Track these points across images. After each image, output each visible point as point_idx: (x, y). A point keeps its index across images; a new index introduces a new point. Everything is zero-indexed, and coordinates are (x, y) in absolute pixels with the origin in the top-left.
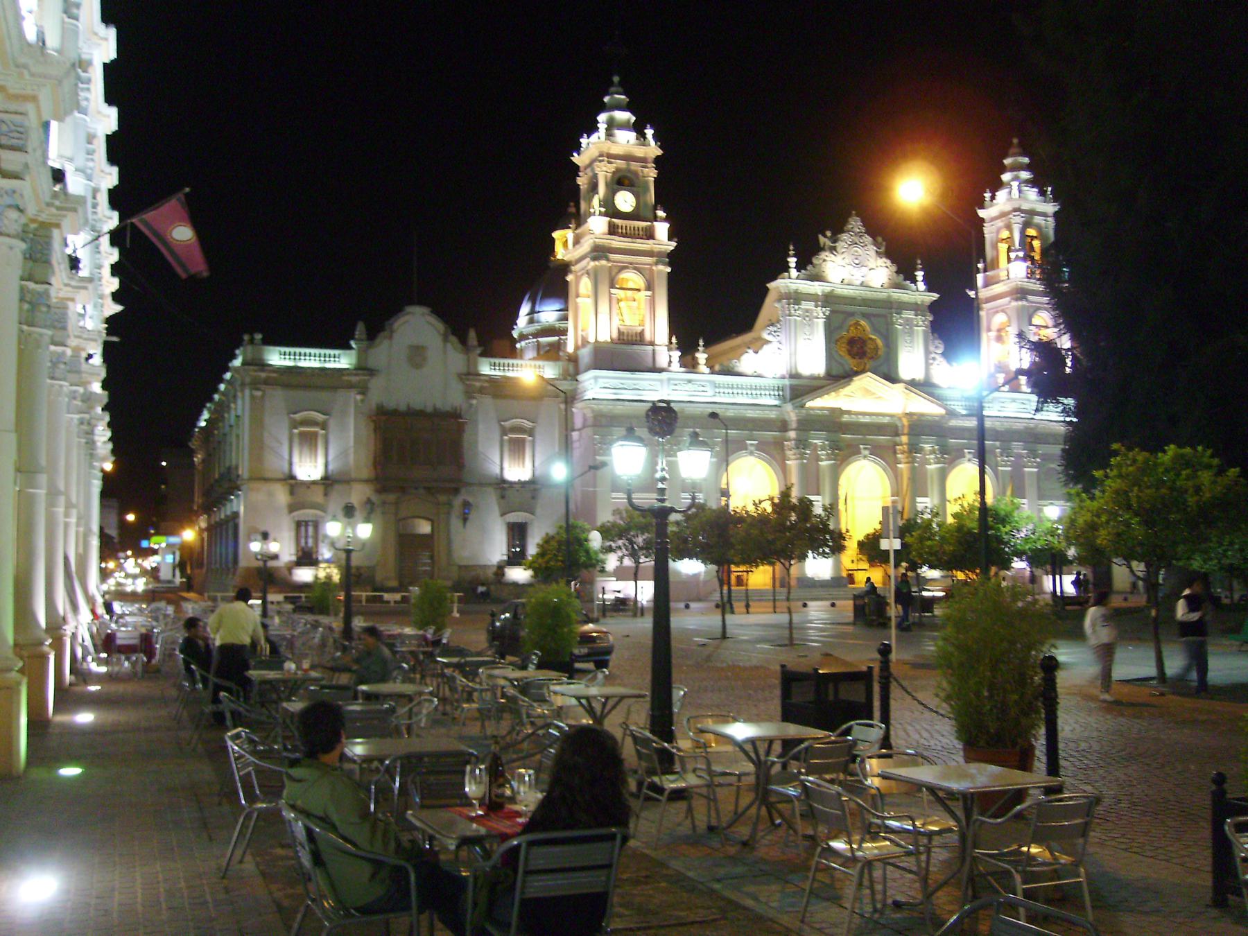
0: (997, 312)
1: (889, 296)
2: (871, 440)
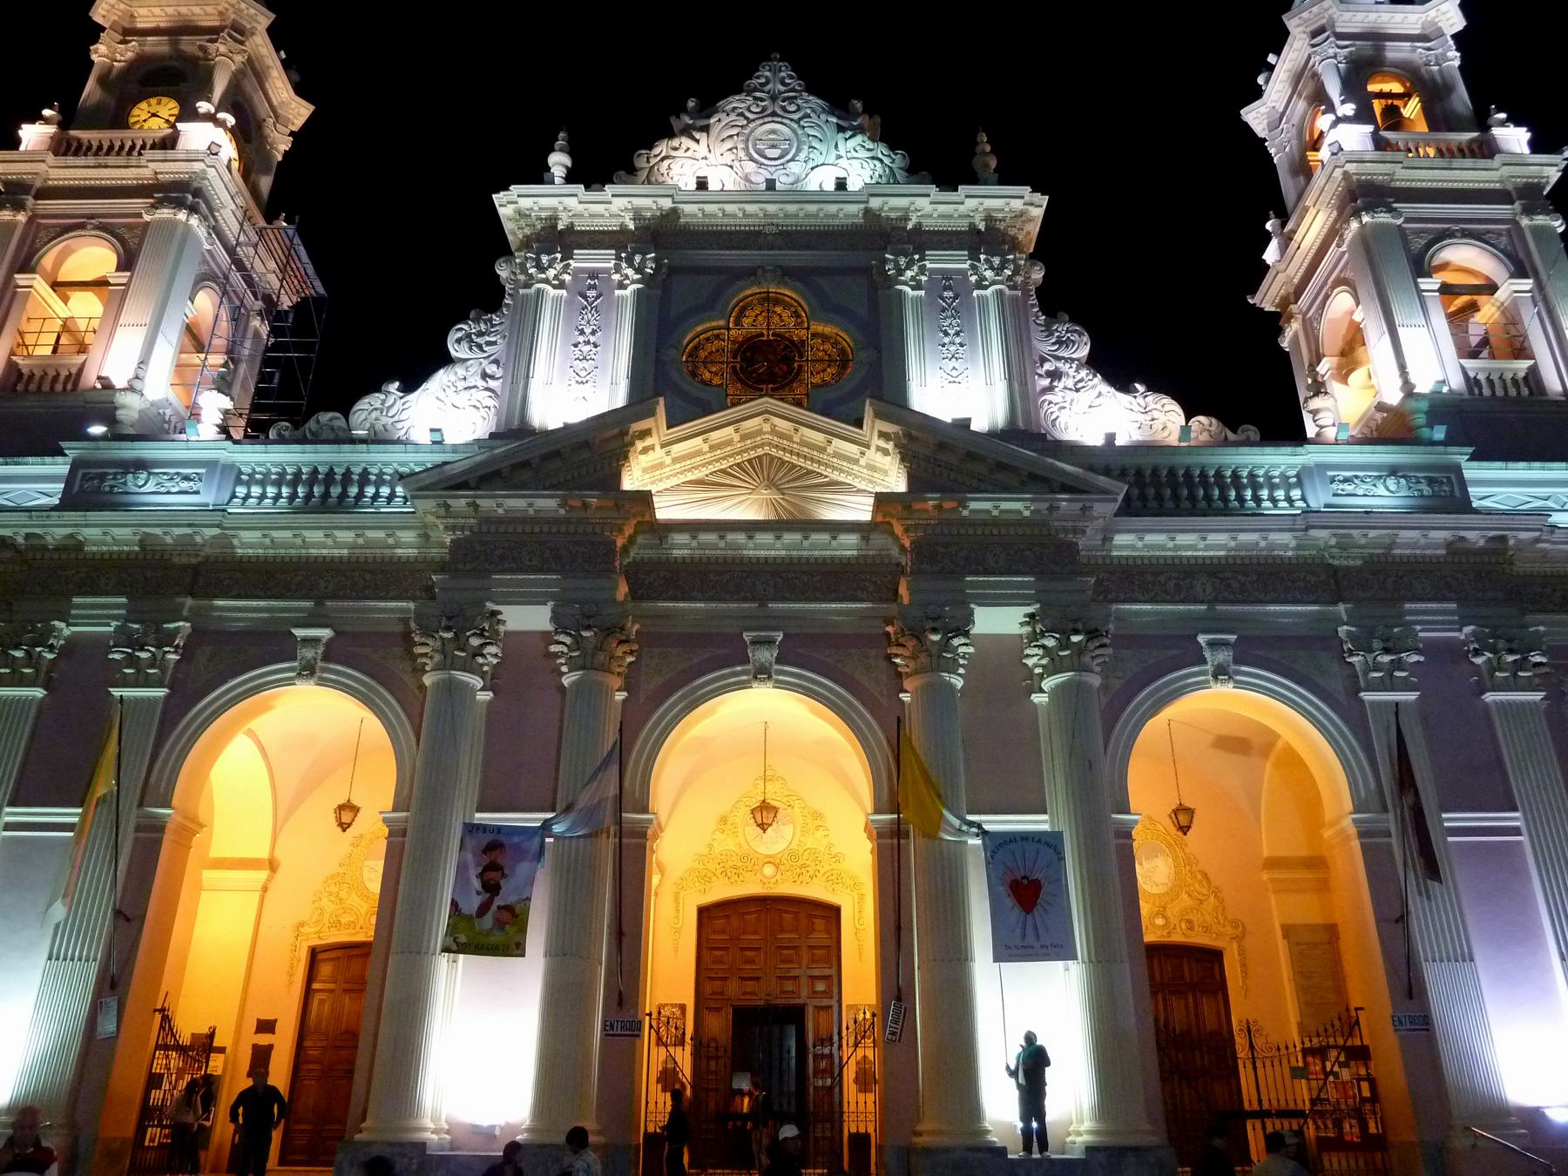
0: (1327, 297)
1: (867, 211)
2: (794, 616)
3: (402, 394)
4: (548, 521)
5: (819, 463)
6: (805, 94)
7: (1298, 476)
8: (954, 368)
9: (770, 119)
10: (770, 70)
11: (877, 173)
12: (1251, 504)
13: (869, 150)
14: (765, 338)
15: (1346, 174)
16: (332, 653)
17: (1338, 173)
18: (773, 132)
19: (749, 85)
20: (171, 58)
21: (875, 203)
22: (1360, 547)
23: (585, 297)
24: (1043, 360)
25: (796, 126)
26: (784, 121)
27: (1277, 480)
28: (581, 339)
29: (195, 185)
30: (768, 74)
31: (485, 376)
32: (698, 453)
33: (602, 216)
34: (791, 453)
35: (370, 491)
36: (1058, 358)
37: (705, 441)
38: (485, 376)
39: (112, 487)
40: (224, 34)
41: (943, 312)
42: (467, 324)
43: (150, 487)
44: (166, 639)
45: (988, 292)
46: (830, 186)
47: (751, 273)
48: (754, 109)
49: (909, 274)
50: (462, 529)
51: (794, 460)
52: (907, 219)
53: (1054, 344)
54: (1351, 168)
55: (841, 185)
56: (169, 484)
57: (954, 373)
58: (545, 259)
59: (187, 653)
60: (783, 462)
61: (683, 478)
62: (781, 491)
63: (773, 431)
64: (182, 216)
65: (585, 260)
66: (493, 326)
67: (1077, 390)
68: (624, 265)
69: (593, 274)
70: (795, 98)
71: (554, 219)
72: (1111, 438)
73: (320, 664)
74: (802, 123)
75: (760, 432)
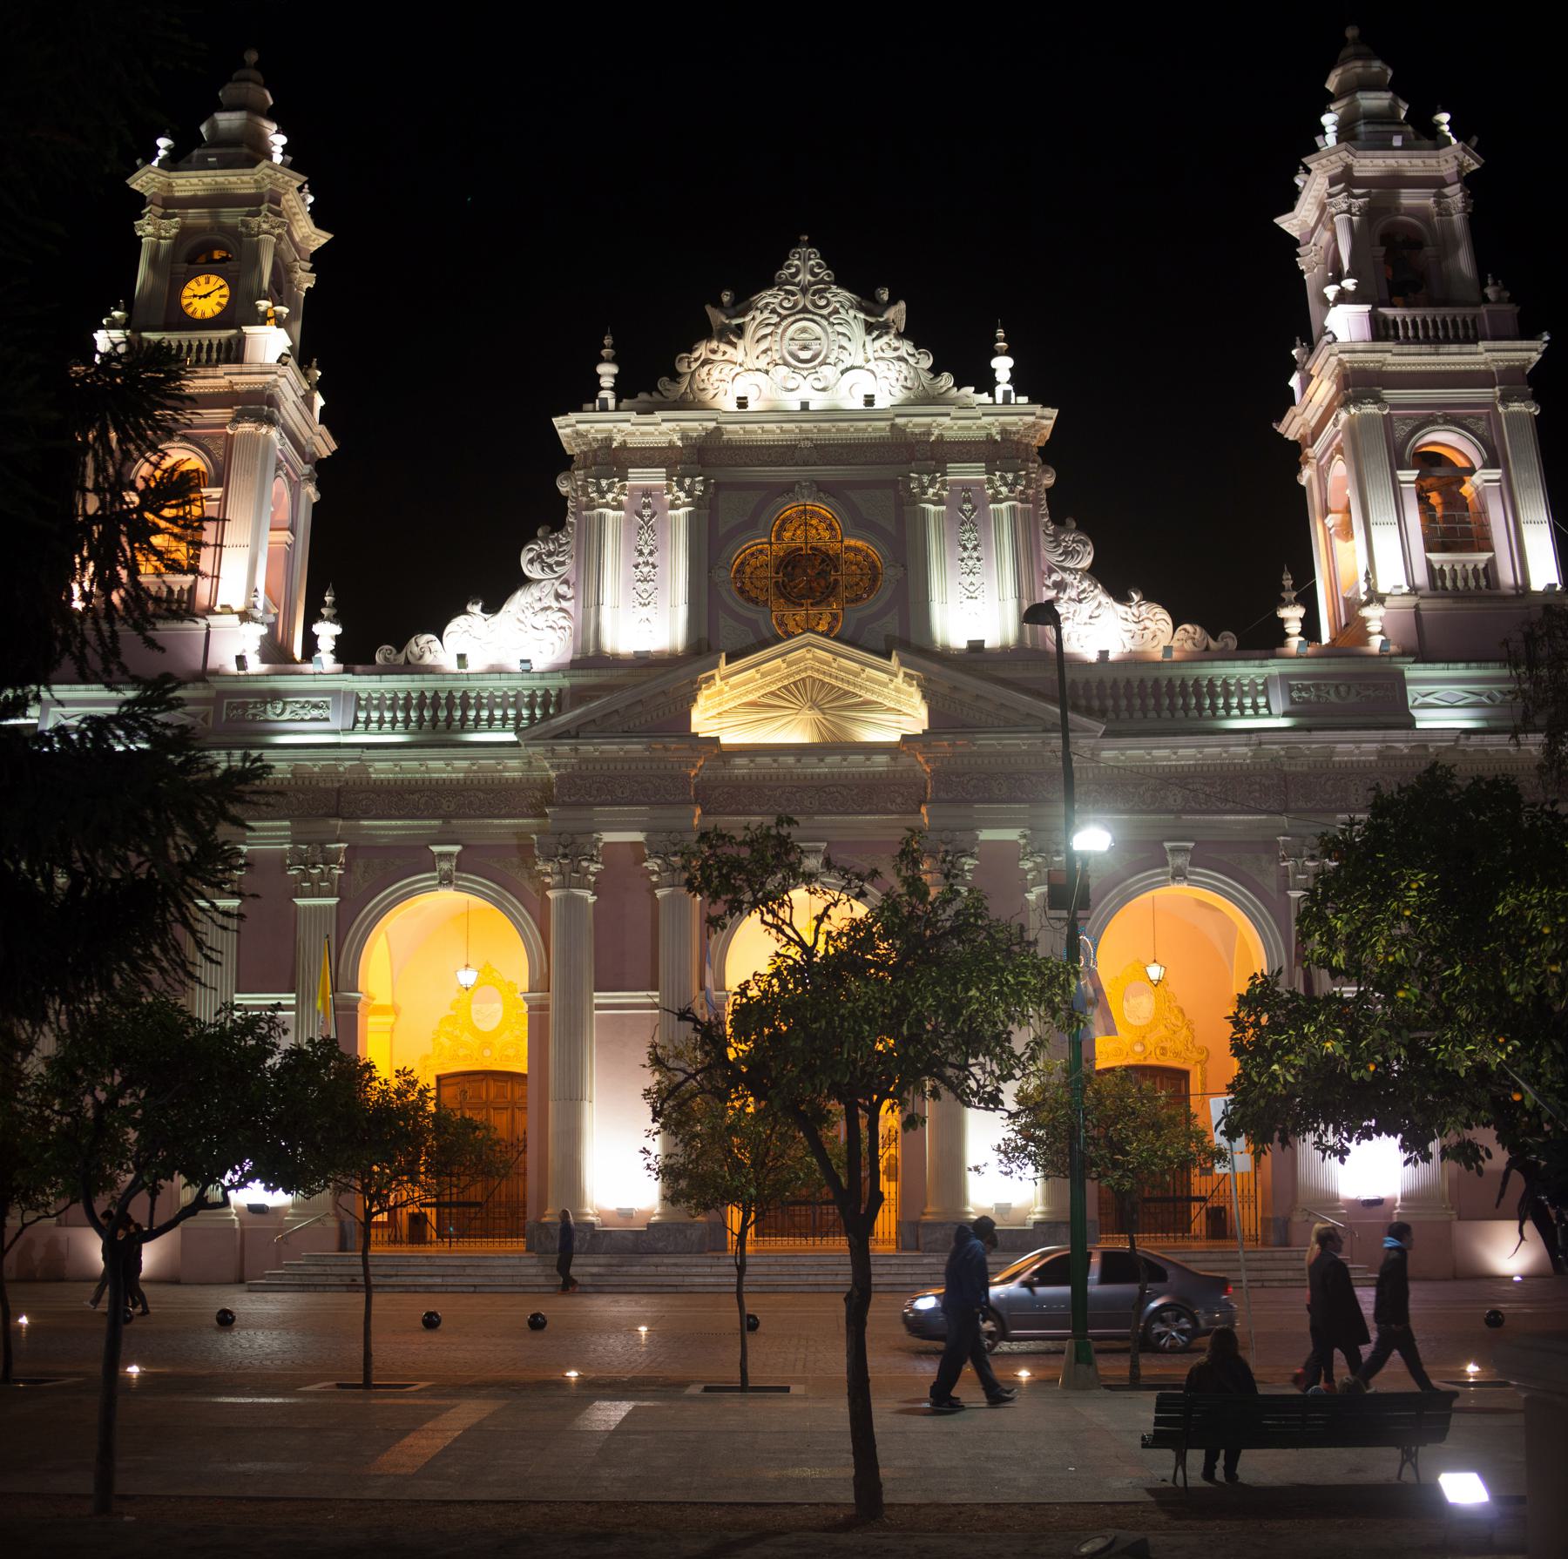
1: (893, 426)
3: (487, 616)
4: (633, 760)
5: (855, 685)
6: (834, 287)
7: (1265, 684)
8: (972, 584)
9: (801, 316)
10: (799, 259)
11: (902, 376)
12: (1222, 712)
13: (896, 349)
14: (803, 552)
15: (1340, 360)
16: (465, 864)
17: (1333, 360)
18: (804, 330)
19: (780, 277)
20: (212, 229)
21: (900, 421)
22: (1306, 756)
23: (641, 516)
24: (1051, 571)
25: (825, 323)
26: (816, 318)
27: (1246, 689)
28: (641, 560)
29: (268, 392)
30: (796, 262)
31: (558, 597)
32: (752, 680)
33: (652, 434)
34: (830, 676)
35: (472, 714)
36: (1064, 569)
37: (757, 671)
38: (558, 597)
39: (254, 715)
40: (264, 207)
41: (962, 524)
42: (536, 544)
43: (286, 716)
44: (329, 859)
45: (1004, 506)
46: (859, 404)
47: (788, 489)
48: (786, 304)
49: (931, 491)
50: (566, 766)
51: (833, 682)
52: (929, 434)
53: (1061, 555)
54: (1345, 357)
55: (869, 400)
56: (301, 712)
57: (972, 588)
58: (604, 483)
59: (347, 867)
60: (824, 683)
61: (739, 701)
62: (823, 711)
63: (815, 658)
64: (264, 430)
65: (640, 478)
66: (561, 545)
67: (1080, 601)
68: (675, 489)
69: (647, 492)
70: (824, 290)
71: (610, 439)
72: (1104, 654)
73: (455, 874)
74: (831, 319)
75: (802, 659)
